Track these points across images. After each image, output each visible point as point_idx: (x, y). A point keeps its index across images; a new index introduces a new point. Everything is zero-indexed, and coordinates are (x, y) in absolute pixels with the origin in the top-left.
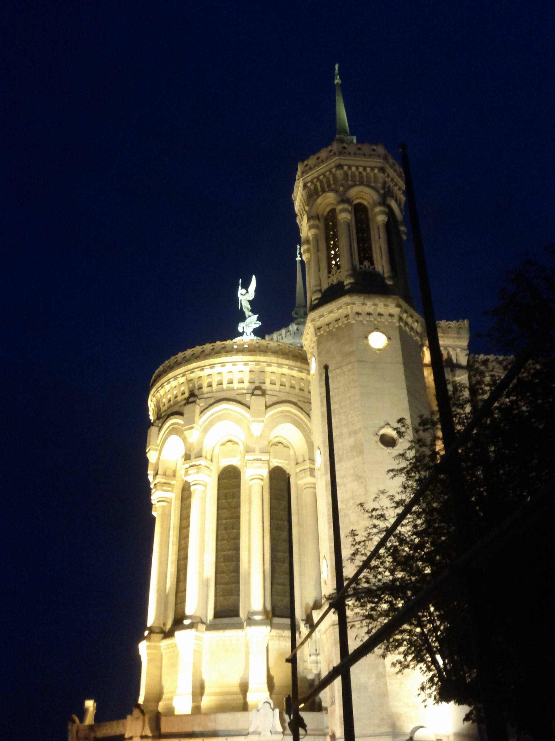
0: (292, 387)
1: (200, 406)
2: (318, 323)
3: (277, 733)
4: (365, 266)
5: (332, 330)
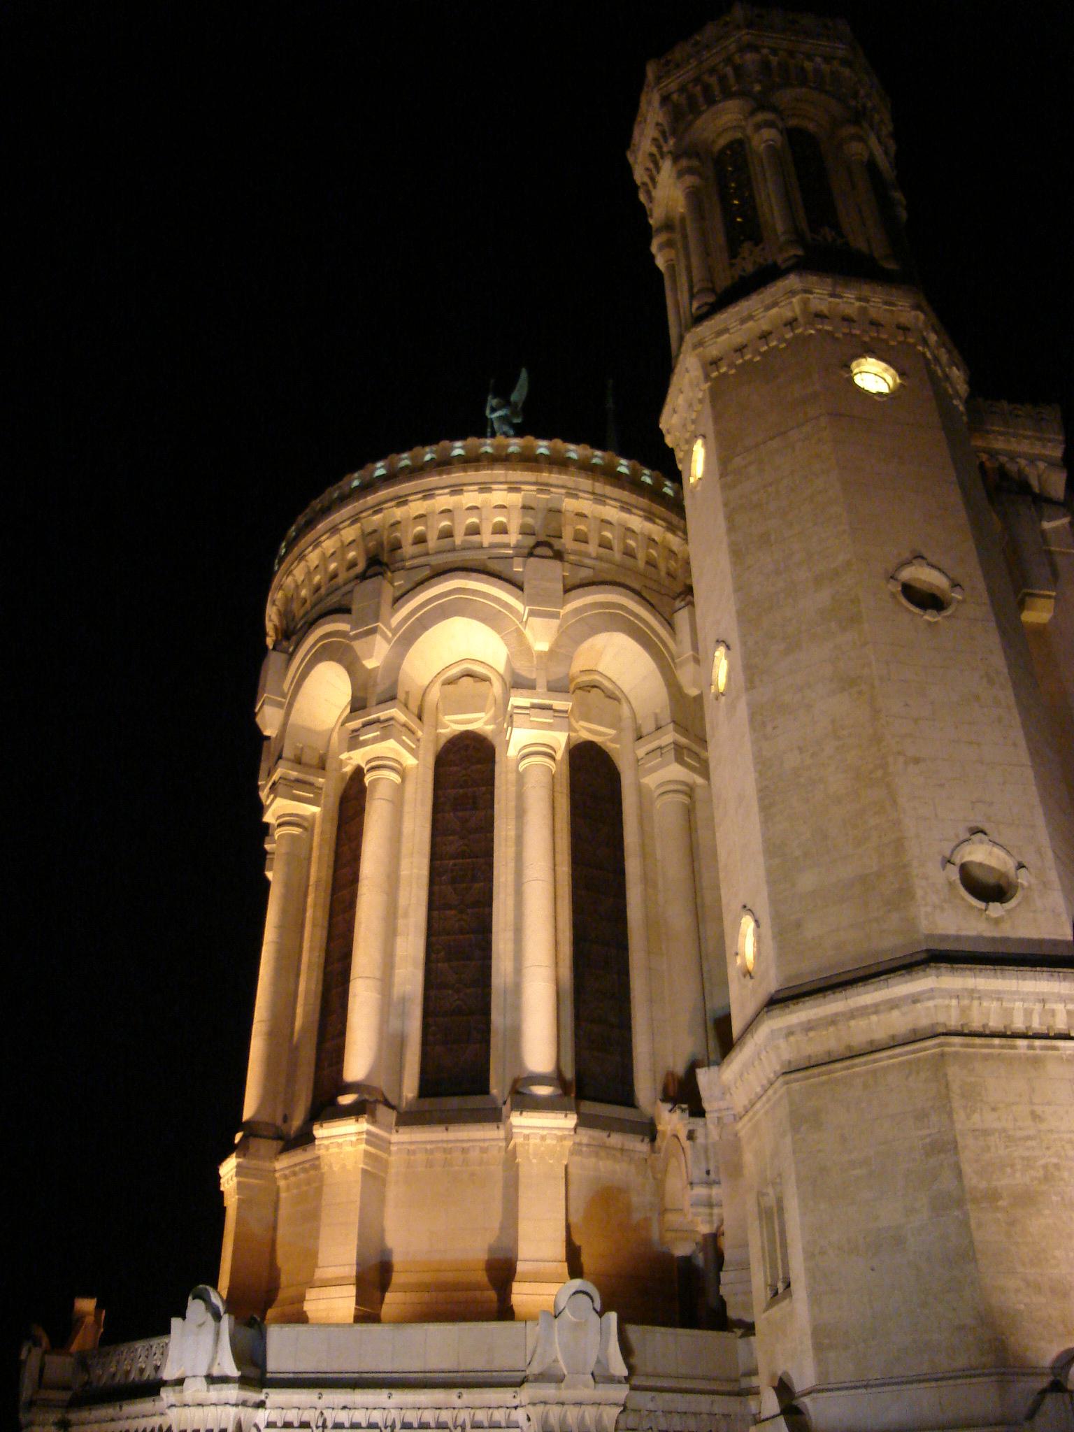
0: (629, 553)
1: (393, 586)
2: (713, 351)
3: (611, 1380)
5: (751, 361)
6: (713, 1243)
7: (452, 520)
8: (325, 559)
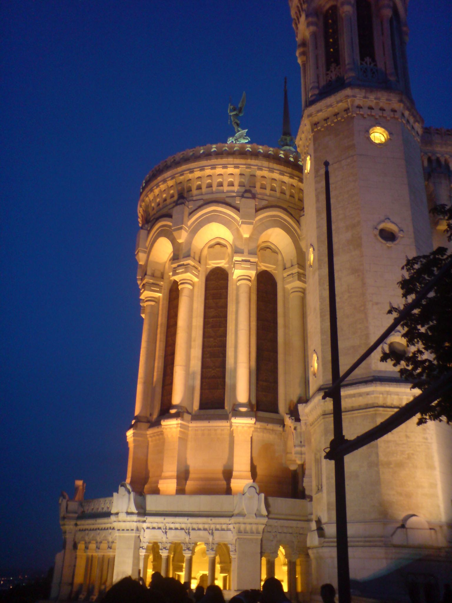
0: (283, 192)
1: (189, 208)
2: (315, 119)
3: (262, 516)
4: (366, 63)
5: (330, 125)
6: (302, 467)
7: (212, 180)
8: (161, 192)
